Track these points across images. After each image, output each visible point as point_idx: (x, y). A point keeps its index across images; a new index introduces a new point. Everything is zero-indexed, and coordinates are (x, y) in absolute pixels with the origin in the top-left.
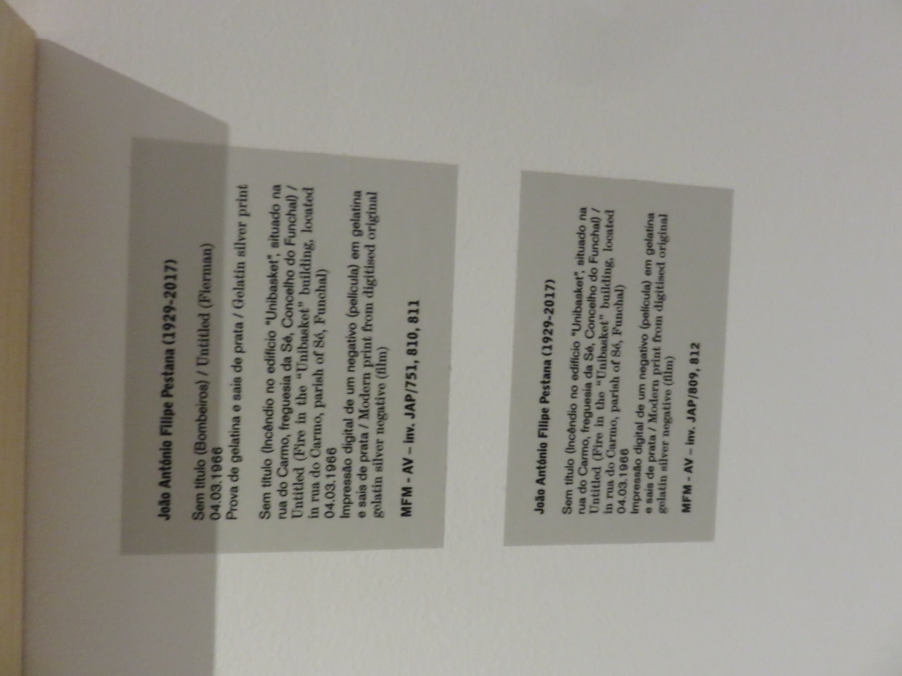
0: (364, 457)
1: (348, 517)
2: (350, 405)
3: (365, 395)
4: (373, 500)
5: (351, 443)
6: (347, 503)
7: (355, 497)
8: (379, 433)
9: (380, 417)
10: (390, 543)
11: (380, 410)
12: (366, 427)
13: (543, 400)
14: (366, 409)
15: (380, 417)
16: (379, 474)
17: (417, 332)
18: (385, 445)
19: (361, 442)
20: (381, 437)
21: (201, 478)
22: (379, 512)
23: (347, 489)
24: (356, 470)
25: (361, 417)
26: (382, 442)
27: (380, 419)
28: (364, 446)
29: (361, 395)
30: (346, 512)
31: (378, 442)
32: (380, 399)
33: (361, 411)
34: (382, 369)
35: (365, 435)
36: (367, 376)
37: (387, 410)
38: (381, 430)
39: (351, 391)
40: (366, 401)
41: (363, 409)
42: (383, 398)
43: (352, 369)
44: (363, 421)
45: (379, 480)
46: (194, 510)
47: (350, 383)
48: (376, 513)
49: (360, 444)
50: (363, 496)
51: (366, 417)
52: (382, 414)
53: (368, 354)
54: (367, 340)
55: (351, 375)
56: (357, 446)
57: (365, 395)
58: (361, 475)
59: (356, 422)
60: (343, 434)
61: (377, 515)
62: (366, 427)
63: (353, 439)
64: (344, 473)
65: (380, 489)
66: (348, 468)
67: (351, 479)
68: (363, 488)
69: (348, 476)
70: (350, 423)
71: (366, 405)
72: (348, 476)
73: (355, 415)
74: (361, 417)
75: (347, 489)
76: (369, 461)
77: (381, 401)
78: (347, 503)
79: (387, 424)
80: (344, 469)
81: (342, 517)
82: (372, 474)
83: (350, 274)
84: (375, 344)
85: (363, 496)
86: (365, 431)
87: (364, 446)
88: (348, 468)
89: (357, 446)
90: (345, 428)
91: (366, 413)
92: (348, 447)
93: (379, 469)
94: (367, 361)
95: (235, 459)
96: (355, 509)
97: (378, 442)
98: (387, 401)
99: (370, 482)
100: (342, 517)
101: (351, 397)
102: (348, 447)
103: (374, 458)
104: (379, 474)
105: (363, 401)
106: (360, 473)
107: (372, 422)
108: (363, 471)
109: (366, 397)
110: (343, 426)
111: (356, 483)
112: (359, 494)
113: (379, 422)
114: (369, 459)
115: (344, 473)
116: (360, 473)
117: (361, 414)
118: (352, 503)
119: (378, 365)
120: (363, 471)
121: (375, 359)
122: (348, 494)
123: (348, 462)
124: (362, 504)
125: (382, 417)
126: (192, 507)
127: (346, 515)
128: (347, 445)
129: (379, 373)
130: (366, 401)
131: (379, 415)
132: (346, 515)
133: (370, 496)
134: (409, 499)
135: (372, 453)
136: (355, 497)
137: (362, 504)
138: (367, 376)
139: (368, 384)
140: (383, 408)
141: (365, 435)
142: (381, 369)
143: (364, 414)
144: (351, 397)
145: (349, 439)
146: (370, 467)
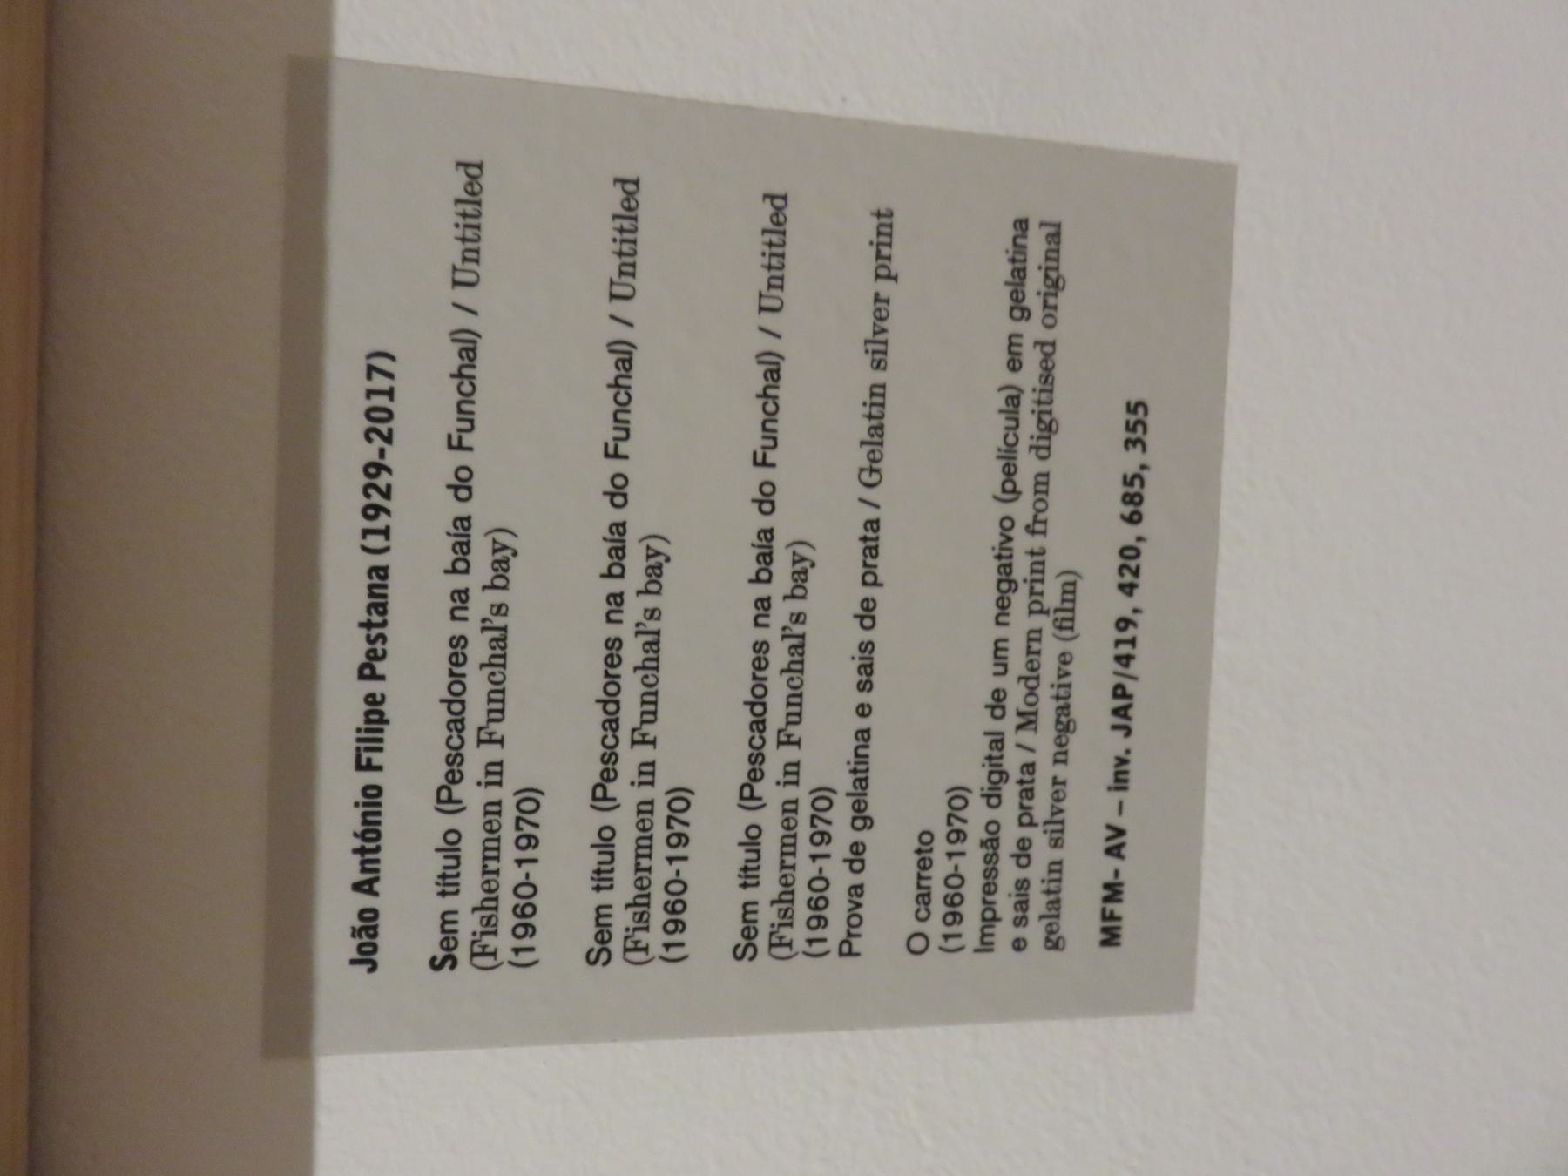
0: (1026, 817)
1: (992, 950)
2: (997, 702)
3: (1031, 678)
4: (1045, 912)
5: (1001, 785)
6: (990, 919)
7: (1005, 904)
8: (1056, 761)
9: (1060, 727)
10: (1002, 1010)
11: (1059, 711)
12: (1032, 750)
13: (367, 672)
14: (1032, 709)
15: (1060, 727)
16: (1057, 854)
17: (1141, 545)
18: (1069, 789)
19: (1021, 782)
20: (1061, 771)
21: (607, 867)
22: (1054, 937)
23: (989, 889)
24: (1008, 846)
25: (1020, 727)
26: (1064, 783)
27: (1063, 730)
28: (1028, 793)
29: (1020, 678)
30: (987, 939)
31: (1055, 781)
32: (1060, 686)
33: (1020, 714)
34: (1065, 623)
35: (1029, 768)
36: (1034, 636)
37: (1075, 712)
38: (1061, 757)
39: (1001, 669)
40: (1032, 691)
41: (1024, 708)
42: (1069, 686)
43: (1002, 619)
44: (1026, 737)
45: (1056, 867)
46: (592, 943)
47: (999, 650)
48: (1048, 940)
49: (1018, 788)
50: (1022, 904)
51: (1033, 726)
52: (1064, 719)
53: (1038, 587)
54: (1037, 555)
55: (1001, 632)
56: (1010, 792)
57: (1031, 678)
58: (1018, 857)
59: (1011, 739)
60: (984, 765)
61: (1050, 944)
62: (1032, 750)
63: (1004, 776)
64: (983, 852)
65: (1058, 887)
66: (991, 842)
67: (999, 866)
68: (1022, 885)
69: (991, 860)
70: (997, 741)
71: (1031, 699)
72: (991, 860)
73: (1009, 724)
74: (1020, 727)
75: (989, 889)
76: (1036, 825)
77: (1062, 692)
78: (990, 919)
79: (1075, 743)
80: (983, 844)
81: (976, 951)
82: (1042, 853)
83: (1003, 406)
84: (1053, 564)
85: (1022, 904)
86: (1028, 757)
87: (1028, 793)
88: (991, 842)
89: (1010, 792)
90: (987, 752)
91: (1032, 718)
92: (992, 796)
93: (1056, 843)
94: (1035, 602)
95: (859, 823)
96: (1004, 932)
97: (1055, 781)
98: (1075, 691)
99: (1037, 872)
100: (976, 951)
101: (1000, 682)
102: (992, 796)
103: (1047, 816)
104: (1057, 854)
105: (1026, 691)
106: (1015, 850)
107: (1043, 739)
108: (1024, 846)
109: (1032, 683)
110: (983, 746)
111: (1008, 873)
112: (1014, 899)
113: (1059, 737)
114: (1035, 821)
115: (983, 852)
116: (1015, 850)
117: (1021, 720)
118: (999, 920)
119: (1056, 610)
120: (1024, 846)
121: (1052, 598)
122: (989, 898)
123: (993, 828)
124: (1020, 922)
125: (1065, 727)
126: (732, 933)
127: (986, 946)
128: (990, 789)
129: (1061, 628)
130: (1032, 691)
131: (1058, 722)
132: (986, 946)
133: (1038, 903)
134: (1117, 908)
135: (1041, 807)
136: (1005, 904)
137: (1020, 922)
138: (1034, 636)
139: (1038, 653)
140: (1067, 707)
141: (1029, 768)
142: (1064, 619)
143: (1028, 720)
144: (1000, 682)
145: (995, 777)
146: (1039, 838)
